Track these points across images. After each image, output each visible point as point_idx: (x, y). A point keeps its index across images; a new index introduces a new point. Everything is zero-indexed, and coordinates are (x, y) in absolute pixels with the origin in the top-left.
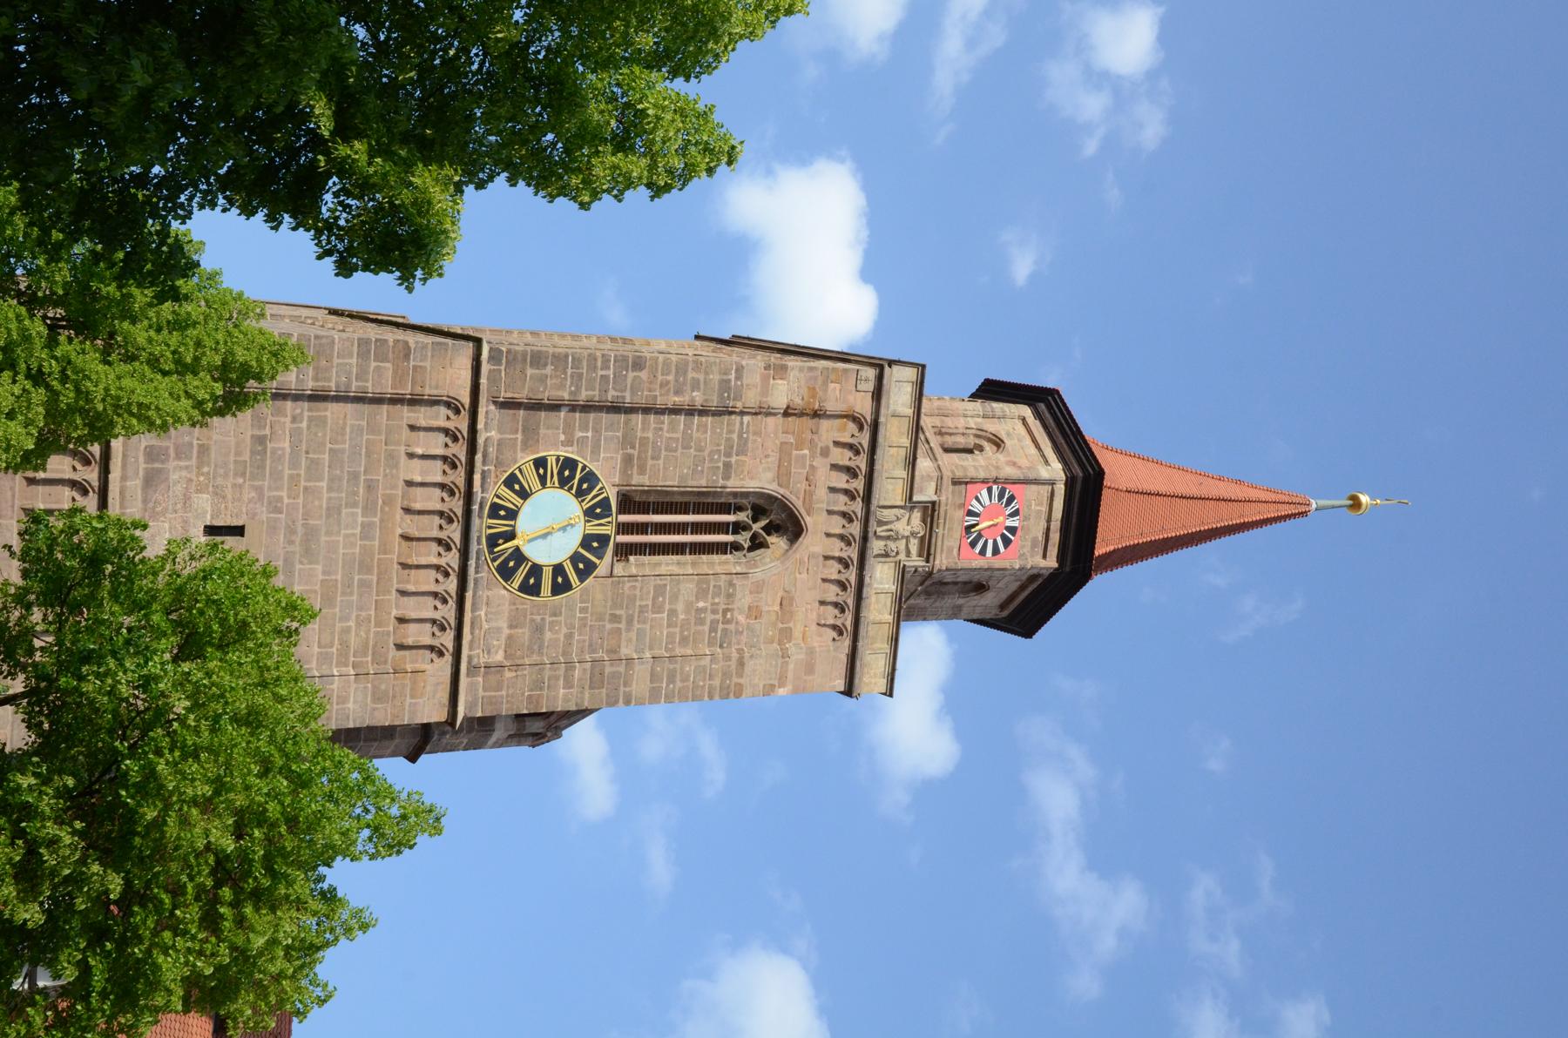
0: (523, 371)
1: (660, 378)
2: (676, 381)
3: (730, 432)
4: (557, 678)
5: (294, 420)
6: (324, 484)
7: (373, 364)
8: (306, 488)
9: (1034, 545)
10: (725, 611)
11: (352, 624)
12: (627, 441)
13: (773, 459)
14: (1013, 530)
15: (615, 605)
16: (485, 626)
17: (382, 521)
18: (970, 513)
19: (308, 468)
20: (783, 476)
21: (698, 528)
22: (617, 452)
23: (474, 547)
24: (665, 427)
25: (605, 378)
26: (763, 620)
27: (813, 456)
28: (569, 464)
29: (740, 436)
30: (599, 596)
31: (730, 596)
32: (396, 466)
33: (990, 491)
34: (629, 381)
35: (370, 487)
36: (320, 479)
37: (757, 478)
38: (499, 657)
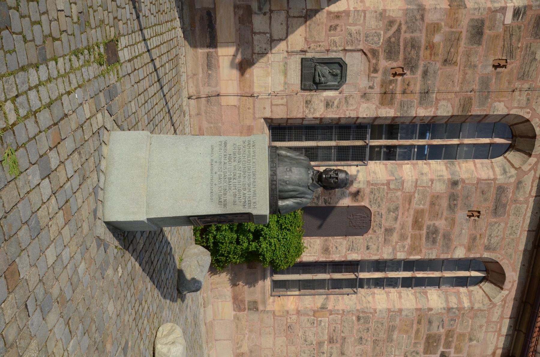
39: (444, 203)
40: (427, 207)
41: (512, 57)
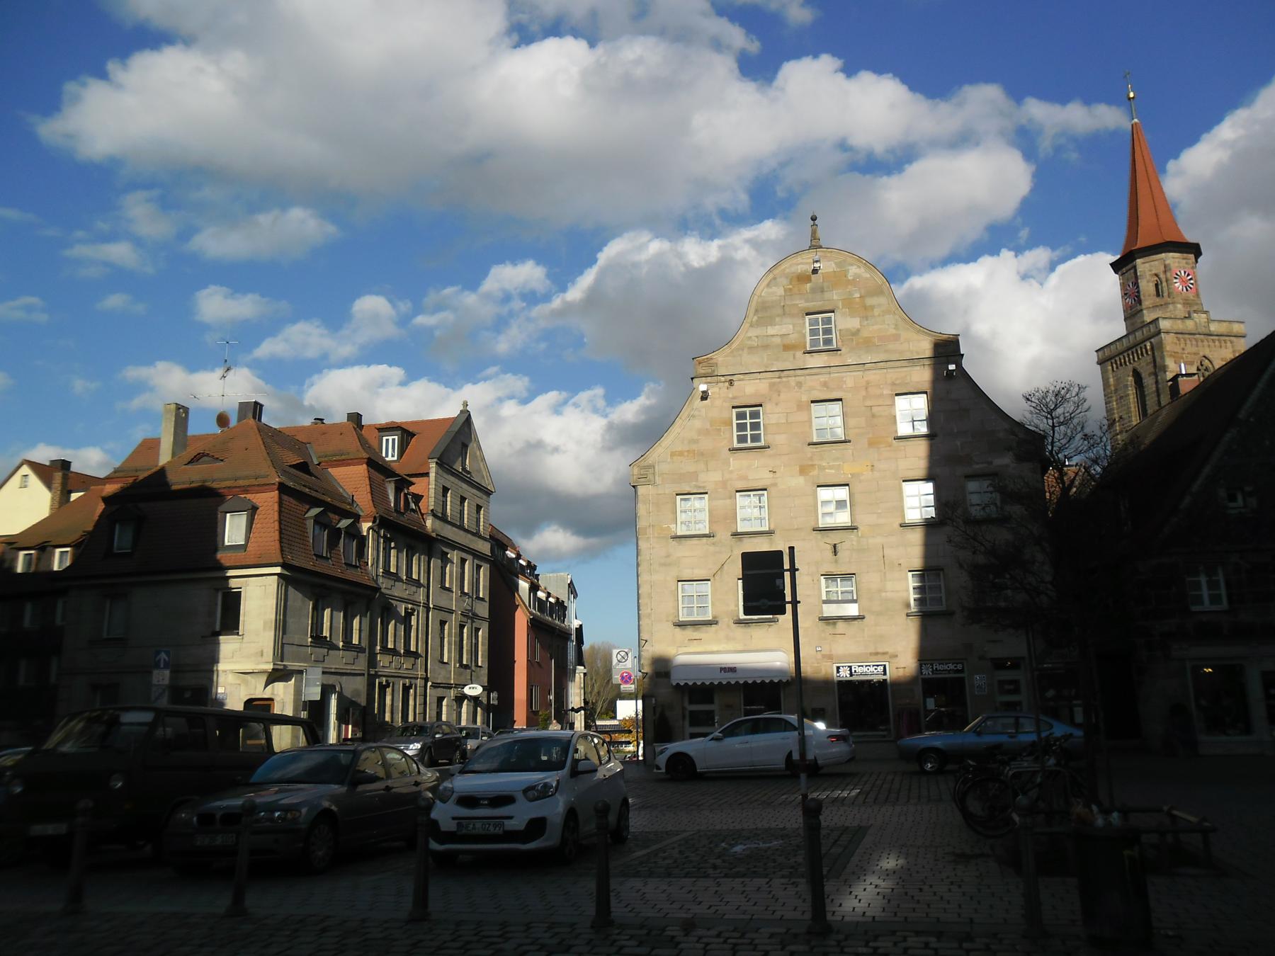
9: (1187, 263)
14: (1185, 272)
33: (1176, 283)
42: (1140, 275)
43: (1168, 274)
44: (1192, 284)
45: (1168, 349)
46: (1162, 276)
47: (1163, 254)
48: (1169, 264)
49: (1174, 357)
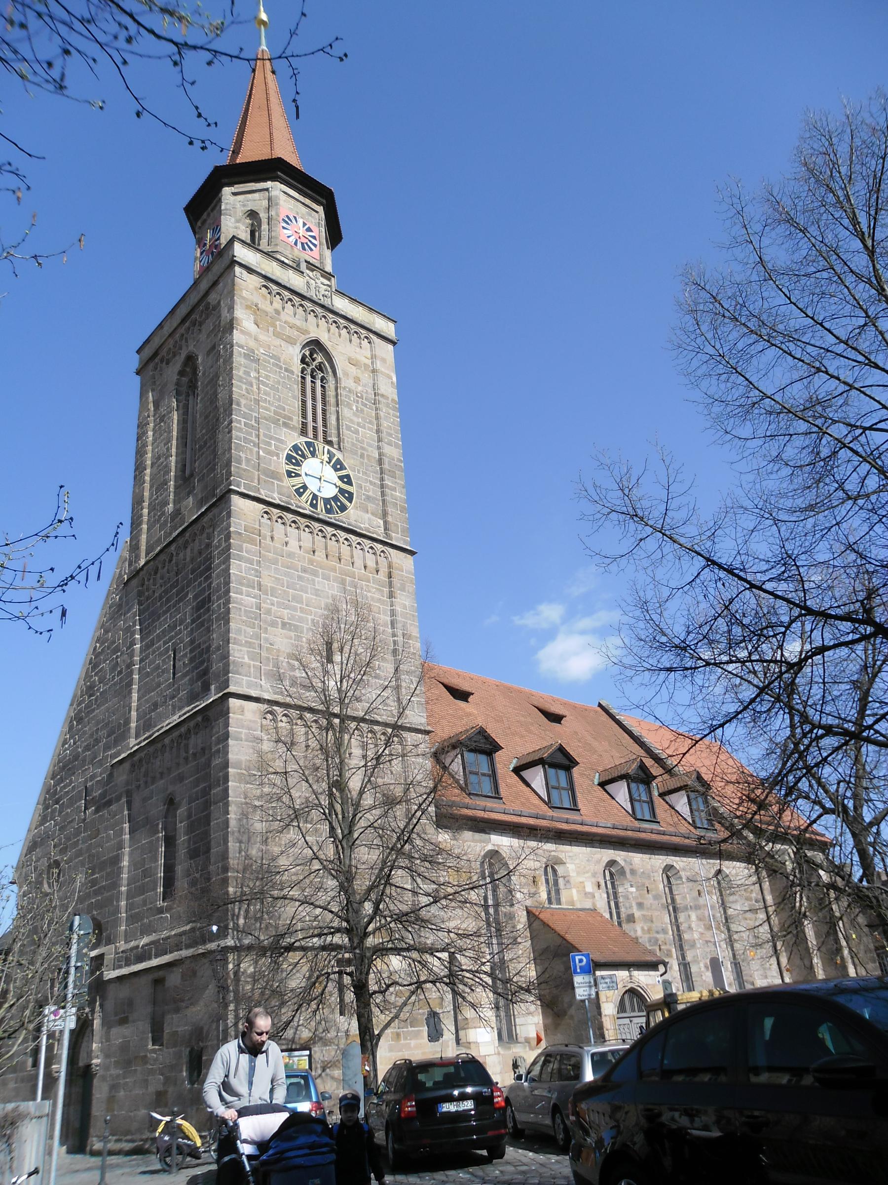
0: (245, 470)
1: (244, 393)
2: (245, 384)
3: (269, 363)
4: (392, 494)
5: (273, 604)
6: (304, 595)
7: (244, 554)
8: (307, 605)
10: (358, 396)
11: (369, 594)
12: (276, 422)
13: (283, 343)
14: (304, 224)
15: (356, 454)
16: (367, 526)
17: (321, 568)
18: (296, 244)
19: (297, 602)
20: (291, 341)
21: (314, 399)
22: (281, 430)
23: (333, 521)
24: (268, 399)
25: (246, 424)
26: (360, 375)
27: (280, 320)
28: (289, 458)
29: (271, 357)
30: (352, 461)
31: (350, 391)
32: (294, 553)
33: (284, 228)
34: (247, 411)
35: (305, 570)
36: (302, 596)
37: (294, 354)
38: (381, 522)
39: (699, 912)
40: (702, 923)
41: (643, 885)
42: (226, 209)
43: (273, 213)
44: (314, 237)
45: (244, 295)
46: (263, 215)
47: (269, 183)
48: (276, 197)
49: (255, 313)
